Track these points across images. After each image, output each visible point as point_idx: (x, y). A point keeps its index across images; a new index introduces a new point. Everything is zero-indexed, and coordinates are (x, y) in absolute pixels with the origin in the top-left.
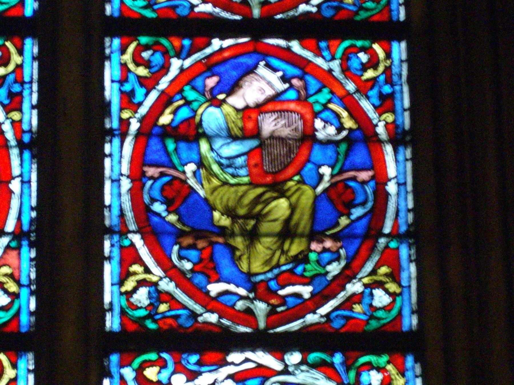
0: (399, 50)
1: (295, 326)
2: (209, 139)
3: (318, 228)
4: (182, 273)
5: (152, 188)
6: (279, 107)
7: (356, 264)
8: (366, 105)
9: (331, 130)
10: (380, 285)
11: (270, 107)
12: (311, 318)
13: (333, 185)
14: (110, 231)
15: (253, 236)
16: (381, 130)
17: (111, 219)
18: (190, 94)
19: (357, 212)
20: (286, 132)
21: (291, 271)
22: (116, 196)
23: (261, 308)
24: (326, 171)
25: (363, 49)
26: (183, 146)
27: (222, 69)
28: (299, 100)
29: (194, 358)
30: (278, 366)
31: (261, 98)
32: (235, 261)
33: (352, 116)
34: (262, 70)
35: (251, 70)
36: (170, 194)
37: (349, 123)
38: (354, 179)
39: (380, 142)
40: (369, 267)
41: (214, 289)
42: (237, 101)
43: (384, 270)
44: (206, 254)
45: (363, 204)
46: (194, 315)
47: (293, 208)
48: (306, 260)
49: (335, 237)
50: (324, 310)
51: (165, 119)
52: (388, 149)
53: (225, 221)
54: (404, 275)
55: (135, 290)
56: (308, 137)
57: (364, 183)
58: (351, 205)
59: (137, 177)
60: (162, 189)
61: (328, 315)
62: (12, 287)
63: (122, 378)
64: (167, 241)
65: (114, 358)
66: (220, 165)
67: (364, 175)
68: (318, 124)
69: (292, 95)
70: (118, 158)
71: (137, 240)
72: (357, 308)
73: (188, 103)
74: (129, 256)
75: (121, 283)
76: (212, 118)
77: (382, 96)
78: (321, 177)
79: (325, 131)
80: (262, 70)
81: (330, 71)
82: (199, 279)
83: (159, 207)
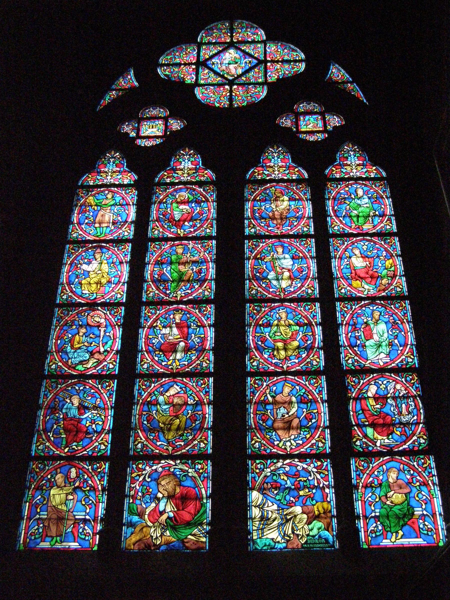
0: (211, 380)
1: (179, 453)
2: (160, 405)
3: (187, 426)
4: (150, 439)
5: (144, 417)
6: (179, 395)
7: (196, 436)
8: (201, 394)
9: (192, 401)
10: (202, 442)
11: (177, 395)
12: (183, 451)
13: (191, 415)
14: (132, 429)
15: (169, 430)
16: (205, 400)
17: (133, 425)
18: (156, 393)
19: (197, 422)
20: (180, 402)
21: (179, 438)
22: (134, 420)
23: (170, 448)
24: (190, 412)
25: (202, 380)
26: (153, 407)
27: (165, 386)
28: (184, 393)
29: (152, 462)
30: (174, 464)
31: (174, 393)
32: (164, 436)
33: (197, 397)
34: (175, 386)
35: (172, 386)
36: (148, 419)
37: (197, 399)
38: (197, 414)
39: (205, 404)
40: (199, 437)
41: (158, 443)
42: (168, 394)
43: (203, 438)
44: (157, 434)
45: (199, 420)
46: (152, 450)
47: (180, 422)
48: (183, 435)
49: (191, 429)
50: (187, 449)
51: (149, 399)
52: (207, 406)
53: (162, 426)
54: (209, 439)
55: (138, 444)
56: (186, 404)
57: (199, 415)
58: (196, 420)
59: (141, 415)
60: (147, 418)
61: (188, 450)
62: (106, 444)
63: (133, 467)
64: (147, 431)
65: (131, 462)
66: (162, 411)
67: (200, 413)
68: (189, 399)
69: (182, 392)
70: (136, 410)
71: (139, 431)
72: (196, 448)
73: (155, 395)
74: (137, 436)
75: (134, 442)
76: (161, 399)
77: (206, 392)
78: (188, 413)
79: (190, 402)
80: (175, 386)
81: (193, 386)
82: (155, 441)
83: (145, 422)
